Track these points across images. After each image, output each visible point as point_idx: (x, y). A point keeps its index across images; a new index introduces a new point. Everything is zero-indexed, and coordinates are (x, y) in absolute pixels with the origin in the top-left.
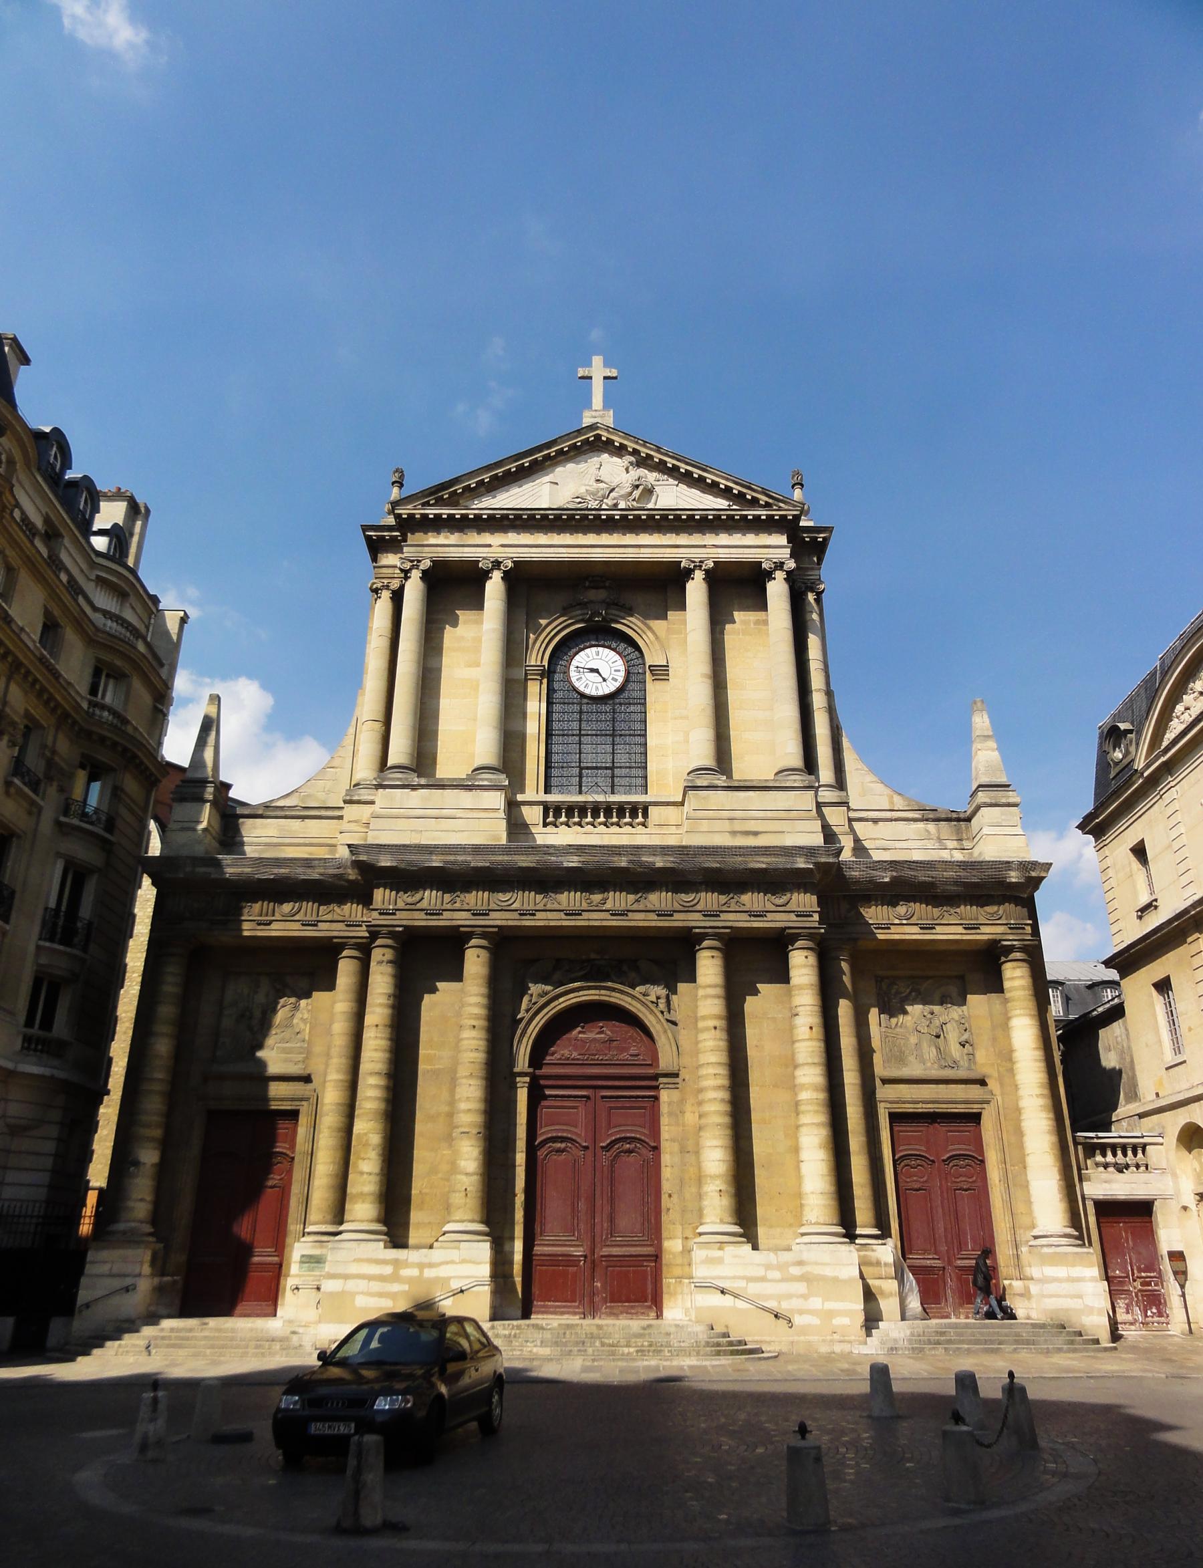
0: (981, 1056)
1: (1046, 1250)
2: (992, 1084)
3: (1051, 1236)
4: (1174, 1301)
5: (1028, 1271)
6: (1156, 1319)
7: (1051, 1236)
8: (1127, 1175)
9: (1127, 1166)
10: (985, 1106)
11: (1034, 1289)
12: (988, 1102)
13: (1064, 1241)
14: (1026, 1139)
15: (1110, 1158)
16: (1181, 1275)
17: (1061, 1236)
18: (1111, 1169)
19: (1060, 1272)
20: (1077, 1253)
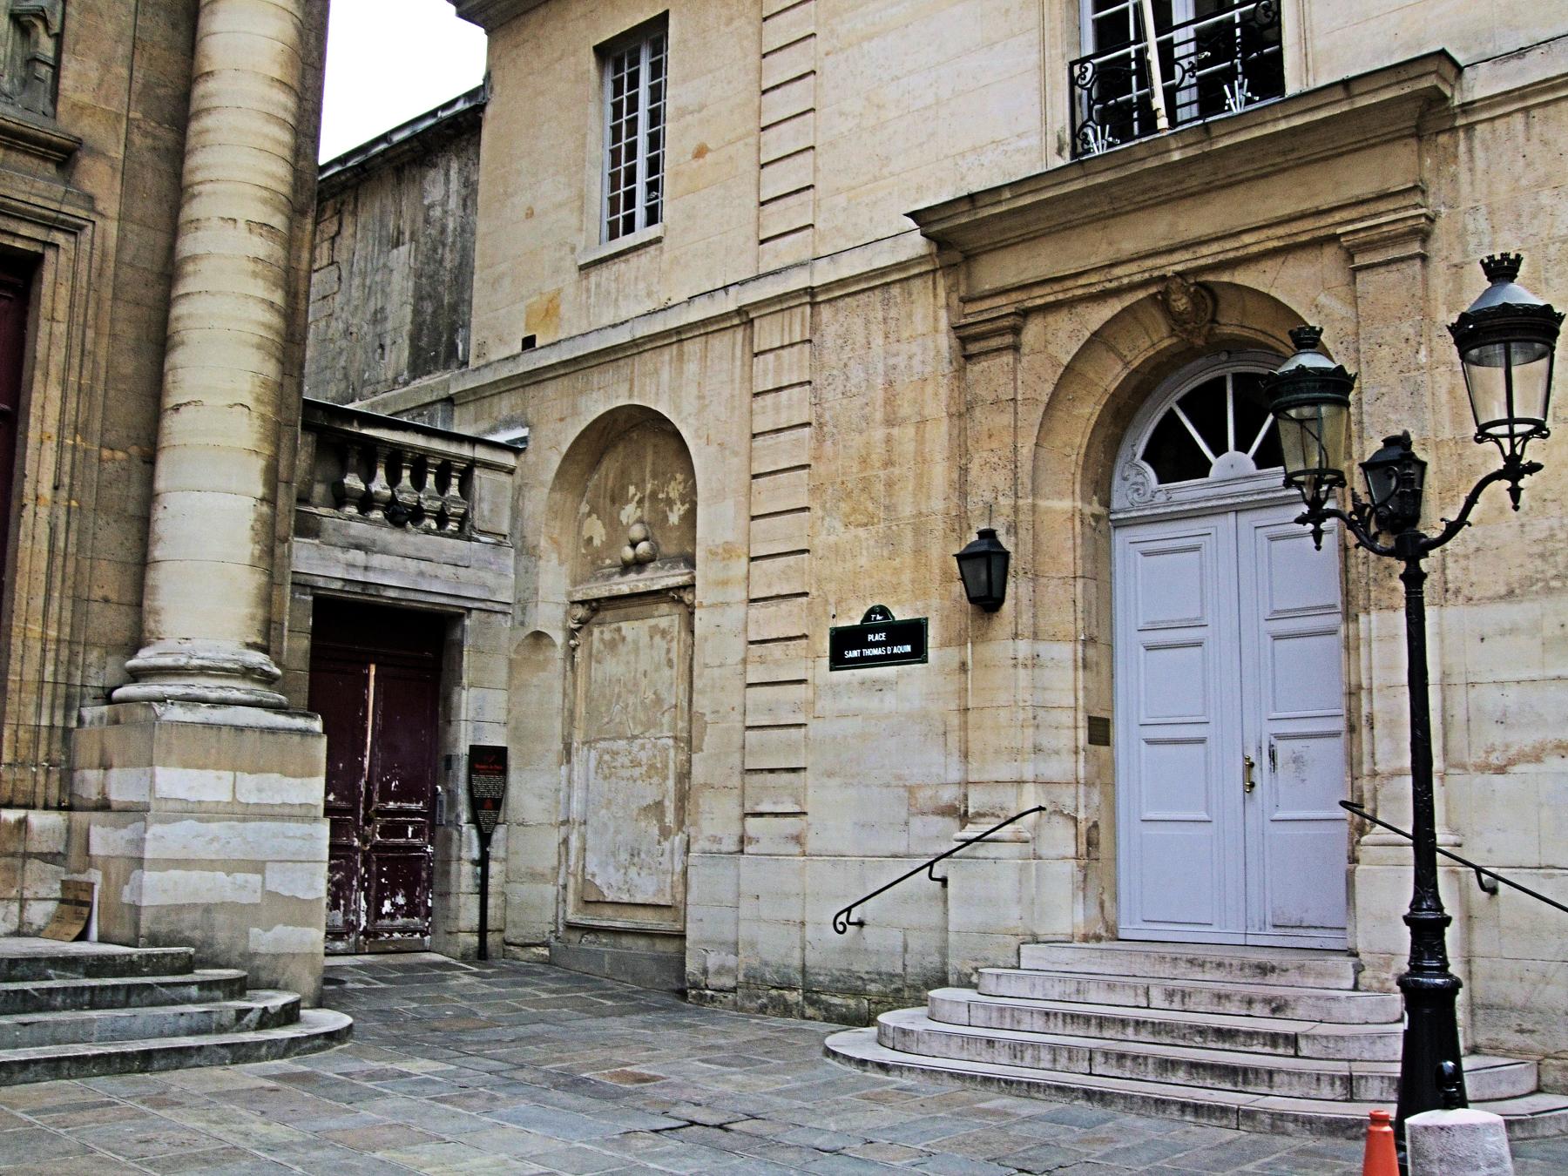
0: (79, 78)
1: (177, 713)
2: (99, 178)
3: (202, 671)
4: (464, 875)
5: (90, 782)
6: (400, 921)
7: (202, 671)
8: (412, 539)
9: (417, 514)
10: (59, 238)
11: (105, 838)
12: (73, 230)
13: (239, 689)
14: (177, 358)
15: (380, 485)
16: (488, 809)
17: (228, 673)
18: (377, 515)
19: (211, 786)
20: (272, 731)
